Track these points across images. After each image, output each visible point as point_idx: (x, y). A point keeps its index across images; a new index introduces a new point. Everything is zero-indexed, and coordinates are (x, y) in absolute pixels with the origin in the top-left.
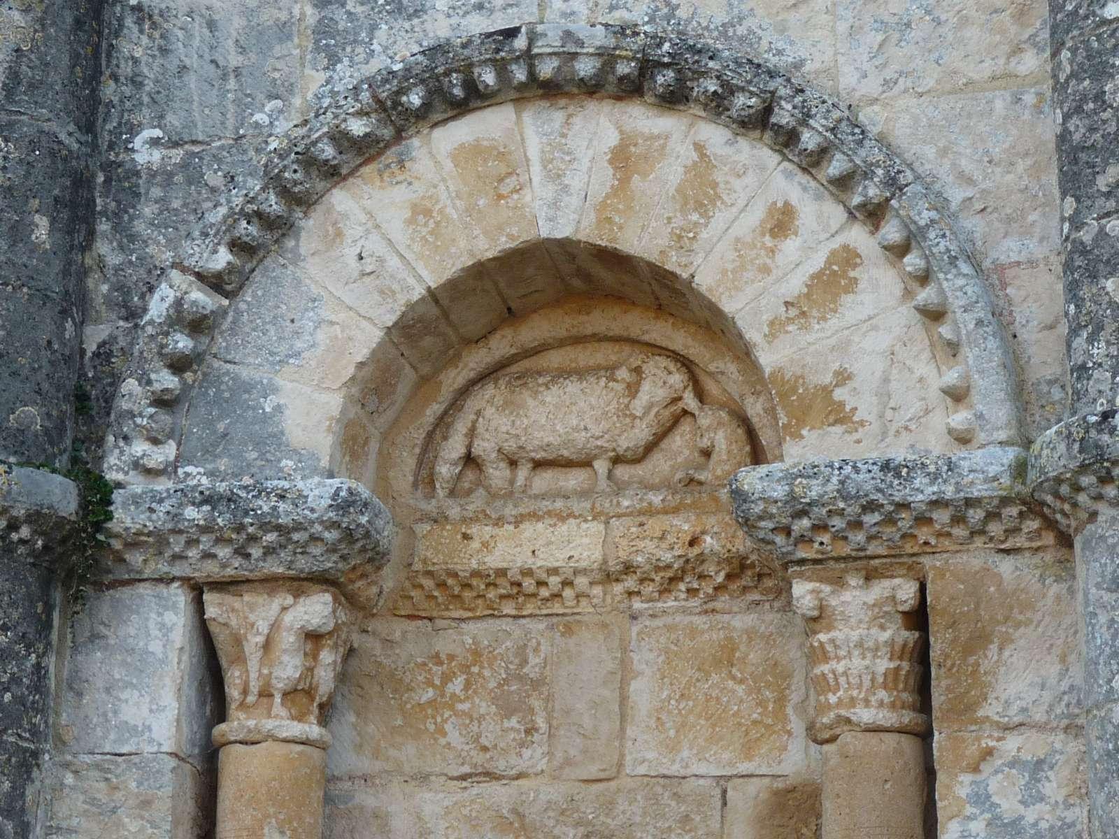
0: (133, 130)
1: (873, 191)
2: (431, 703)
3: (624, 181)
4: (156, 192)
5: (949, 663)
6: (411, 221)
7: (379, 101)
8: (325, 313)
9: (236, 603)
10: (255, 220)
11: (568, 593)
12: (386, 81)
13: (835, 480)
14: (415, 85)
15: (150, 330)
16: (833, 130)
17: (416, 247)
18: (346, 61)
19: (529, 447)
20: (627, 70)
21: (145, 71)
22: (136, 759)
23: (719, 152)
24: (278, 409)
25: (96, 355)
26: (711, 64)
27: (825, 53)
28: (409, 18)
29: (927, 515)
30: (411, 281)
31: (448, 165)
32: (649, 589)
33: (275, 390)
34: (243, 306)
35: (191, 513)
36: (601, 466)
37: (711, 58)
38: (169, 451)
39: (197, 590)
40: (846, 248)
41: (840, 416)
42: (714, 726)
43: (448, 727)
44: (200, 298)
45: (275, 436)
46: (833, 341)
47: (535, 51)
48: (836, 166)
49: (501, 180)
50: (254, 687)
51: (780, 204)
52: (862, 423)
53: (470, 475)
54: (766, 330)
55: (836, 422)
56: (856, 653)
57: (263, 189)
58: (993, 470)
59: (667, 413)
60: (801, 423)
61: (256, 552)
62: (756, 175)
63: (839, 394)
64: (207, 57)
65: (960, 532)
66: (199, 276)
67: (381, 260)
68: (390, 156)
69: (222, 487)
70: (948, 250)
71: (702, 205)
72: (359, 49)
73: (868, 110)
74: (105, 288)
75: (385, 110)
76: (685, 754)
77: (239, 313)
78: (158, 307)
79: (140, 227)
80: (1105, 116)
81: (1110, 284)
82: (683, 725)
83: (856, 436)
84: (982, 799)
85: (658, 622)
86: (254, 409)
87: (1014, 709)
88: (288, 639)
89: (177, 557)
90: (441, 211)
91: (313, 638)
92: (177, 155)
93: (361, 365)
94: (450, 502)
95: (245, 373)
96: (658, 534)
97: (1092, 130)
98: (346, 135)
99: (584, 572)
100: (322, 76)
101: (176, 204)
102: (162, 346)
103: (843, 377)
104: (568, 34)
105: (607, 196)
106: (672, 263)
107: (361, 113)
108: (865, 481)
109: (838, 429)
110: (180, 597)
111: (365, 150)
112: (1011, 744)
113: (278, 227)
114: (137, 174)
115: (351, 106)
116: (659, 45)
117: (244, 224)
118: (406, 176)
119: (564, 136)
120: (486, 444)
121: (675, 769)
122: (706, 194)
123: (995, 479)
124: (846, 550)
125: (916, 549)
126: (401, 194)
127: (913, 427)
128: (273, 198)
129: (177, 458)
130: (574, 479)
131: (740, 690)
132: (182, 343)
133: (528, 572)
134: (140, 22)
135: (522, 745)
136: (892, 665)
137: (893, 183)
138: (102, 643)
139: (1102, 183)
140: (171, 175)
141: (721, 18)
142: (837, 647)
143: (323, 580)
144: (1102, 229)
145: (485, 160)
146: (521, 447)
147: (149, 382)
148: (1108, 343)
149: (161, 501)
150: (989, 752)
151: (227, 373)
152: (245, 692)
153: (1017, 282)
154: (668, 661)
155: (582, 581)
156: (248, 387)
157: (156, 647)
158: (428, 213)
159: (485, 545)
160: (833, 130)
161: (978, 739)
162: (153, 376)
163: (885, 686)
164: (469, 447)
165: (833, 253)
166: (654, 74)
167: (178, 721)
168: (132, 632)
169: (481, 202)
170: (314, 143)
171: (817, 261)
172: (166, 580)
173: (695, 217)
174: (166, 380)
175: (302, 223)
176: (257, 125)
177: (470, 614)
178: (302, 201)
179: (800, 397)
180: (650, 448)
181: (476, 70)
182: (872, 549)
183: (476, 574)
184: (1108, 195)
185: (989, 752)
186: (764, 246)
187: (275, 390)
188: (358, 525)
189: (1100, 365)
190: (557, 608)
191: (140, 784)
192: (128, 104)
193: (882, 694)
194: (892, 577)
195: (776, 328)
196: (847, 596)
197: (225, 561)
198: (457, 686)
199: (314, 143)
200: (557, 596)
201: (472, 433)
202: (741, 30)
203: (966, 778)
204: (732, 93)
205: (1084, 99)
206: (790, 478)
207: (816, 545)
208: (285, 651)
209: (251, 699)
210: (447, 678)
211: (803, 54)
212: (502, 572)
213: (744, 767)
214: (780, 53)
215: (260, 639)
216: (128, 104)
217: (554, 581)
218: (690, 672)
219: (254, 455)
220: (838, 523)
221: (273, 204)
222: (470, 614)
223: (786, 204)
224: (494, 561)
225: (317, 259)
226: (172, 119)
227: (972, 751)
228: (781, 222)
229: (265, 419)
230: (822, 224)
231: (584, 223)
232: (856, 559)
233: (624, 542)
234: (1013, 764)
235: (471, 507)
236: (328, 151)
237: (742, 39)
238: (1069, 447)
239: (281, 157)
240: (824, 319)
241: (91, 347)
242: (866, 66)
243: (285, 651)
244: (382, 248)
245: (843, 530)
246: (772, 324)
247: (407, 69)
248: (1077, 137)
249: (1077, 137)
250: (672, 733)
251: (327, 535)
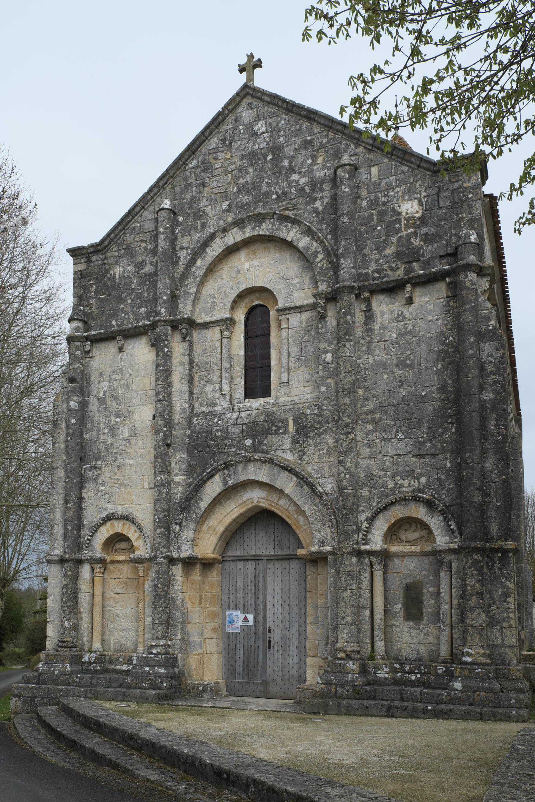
39: (91, 564)
44: (90, 538)
62: (133, 528)
111: (102, 524)
113: (96, 531)
244: (104, 533)
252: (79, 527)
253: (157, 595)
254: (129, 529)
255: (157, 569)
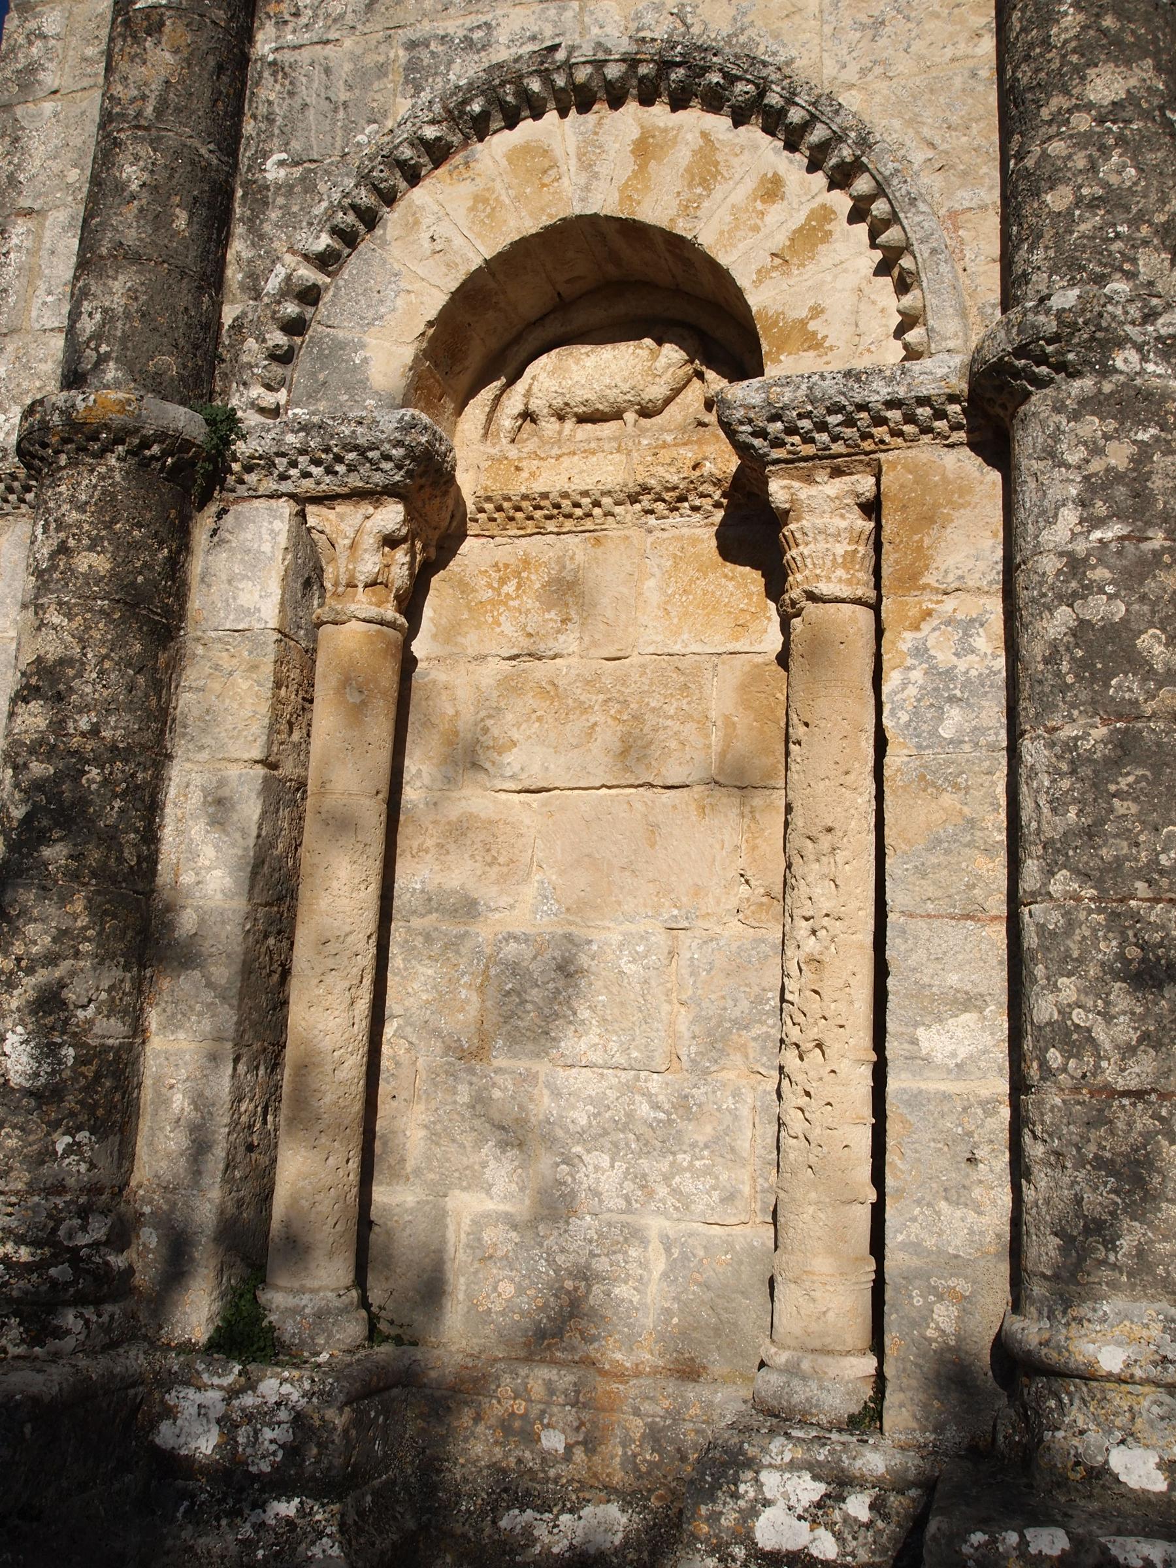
0: (266, 155)
1: (846, 153)
2: (490, 601)
3: (642, 168)
4: (281, 201)
5: (898, 540)
6: (472, 209)
7: (450, 112)
8: (403, 285)
9: (331, 515)
10: (351, 212)
11: (597, 511)
12: (453, 94)
13: (804, 387)
14: (477, 96)
15: (266, 300)
16: (814, 104)
17: (476, 228)
18: (428, 89)
19: (573, 404)
20: (646, 71)
21: (277, 110)
22: (248, 634)
23: (721, 137)
24: (365, 360)
25: (232, 327)
26: (715, 59)
27: (812, 51)
28: (478, 52)
29: (883, 413)
30: (471, 255)
31: (504, 163)
32: (660, 506)
33: (363, 346)
34: (341, 283)
35: (290, 438)
36: (630, 416)
37: (715, 55)
38: (282, 396)
40: (823, 206)
41: (814, 343)
42: (708, 614)
43: (502, 619)
44: (308, 274)
45: (361, 381)
46: (809, 283)
47: (573, 60)
48: (818, 134)
49: (545, 172)
50: (343, 580)
51: (770, 175)
52: (831, 348)
53: (528, 426)
54: (754, 277)
55: (810, 348)
56: (820, 538)
57: (356, 186)
58: (940, 372)
59: (681, 372)
60: (780, 350)
61: (341, 468)
63: (812, 326)
64: (323, 95)
65: (909, 429)
66: (306, 257)
67: (448, 240)
68: (457, 159)
69: (315, 419)
70: (909, 193)
71: (705, 180)
72: (438, 79)
73: (847, 94)
74: (240, 276)
75: (454, 119)
76: (685, 636)
77: (338, 288)
78: (273, 284)
79: (267, 228)
80: (1048, 56)
81: (1049, 198)
82: (686, 614)
83: (826, 359)
84: (920, 652)
85: (665, 535)
86: (347, 361)
87: (951, 577)
88: (369, 541)
89: (283, 477)
90: (497, 199)
91: (390, 541)
92: (297, 172)
93: (430, 324)
94: (511, 446)
95: (340, 334)
96: (668, 461)
97: (1037, 71)
98: (421, 139)
99: (609, 493)
100: (409, 102)
101: (295, 209)
102: (275, 312)
103: (817, 311)
104: (599, 45)
105: (629, 179)
106: (682, 228)
107: (433, 122)
108: (830, 388)
109: (812, 353)
110: (286, 508)
111: (438, 153)
112: (949, 605)
113: (370, 219)
114: (267, 188)
115: (426, 116)
116: (673, 48)
117: (341, 214)
118: (471, 173)
119: (596, 133)
120: (538, 402)
121: (677, 648)
122: (709, 171)
123: (943, 379)
124: (809, 450)
125: (873, 447)
126: (465, 189)
127: (873, 348)
128: (363, 193)
129: (288, 402)
130: (608, 429)
131: (731, 585)
132: (291, 309)
133: (565, 495)
134: (274, 74)
135: (559, 631)
136: (850, 548)
137: (864, 142)
138: (227, 546)
139: (1045, 114)
140: (292, 187)
141: (726, 30)
142: (805, 534)
143: (392, 492)
144: (1044, 152)
145: (533, 157)
146: (567, 404)
147: (264, 341)
148: (1047, 248)
149: (269, 430)
150: (929, 613)
151: (328, 335)
152: (336, 584)
153: (969, 226)
154: (676, 564)
155: (607, 501)
156: (342, 345)
157: (266, 548)
158: (486, 201)
159: (533, 474)
160: (814, 104)
161: (920, 603)
162: (268, 336)
163: (844, 565)
164: (526, 404)
165: (812, 211)
166: (673, 77)
167: (282, 604)
168: (249, 536)
169: (528, 190)
170: (396, 147)
171: (799, 219)
172: (274, 496)
173: (699, 190)
174: (278, 338)
175: (389, 216)
176: (359, 144)
177: (522, 532)
178: (389, 198)
179: (780, 329)
180: (668, 401)
181: (525, 81)
182: (838, 448)
183: (525, 497)
184: (1050, 123)
185: (929, 613)
186: (755, 210)
187: (363, 346)
188: (419, 444)
189: (1039, 268)
190: (588, 524)
191: (251, 653)
192: (263, 136)
193: (840, 572)
194: (852, 474)
195: (762, 275)
196: (813, 490)
197: (320, 481)
198: (510, 588)
199: (396, 147)
200: (589, 515)
201: (528, 394)
202: (742, 39)
203: (908, 635)
204: (732, 83)
205: (1032, 46)
206: (767, 388)
207: (788, 447)
208: (366, 550)
209: (341, 589)
210: (503, 581)
211: (794, 53)
212: (545, 496)
213: (731, 647)
214: (774, 54)
215: (347, 542)
216: (263, 136)
217: (585, 501)
218: (691, 573)
219: (346, 397)
220: (806, 424)
221: (365, 198)
222: (522, 532)
223: (775, 174)
224: (538, 487)
225: (399, 243)
226: (296, 145)
227: (913, 612)
228: (772, 189)
229: (356, 368)
230: (807, 189)
231: (610, 200)
232: (821, 458)
233: (641, 468)
234: (948, 623)
235: (526, 450)
236: (407, 153)
237: (743, 46)
238: (1008, 332)
239: (371, 160)
240: (804, 266)
241: (227, 320)
242: (847, 58)
243: (366, 550)
244: (448, 232)
245: (811, 431)
246: (759, 271)
247: (471, 84)
248: (1025, 81)
249: (1025, 81)
250: (675, 621)
251: (394, 452)
252: (217, 197)
253: (1125, 748)
254: (706, 171)
255: (1119, 456)
